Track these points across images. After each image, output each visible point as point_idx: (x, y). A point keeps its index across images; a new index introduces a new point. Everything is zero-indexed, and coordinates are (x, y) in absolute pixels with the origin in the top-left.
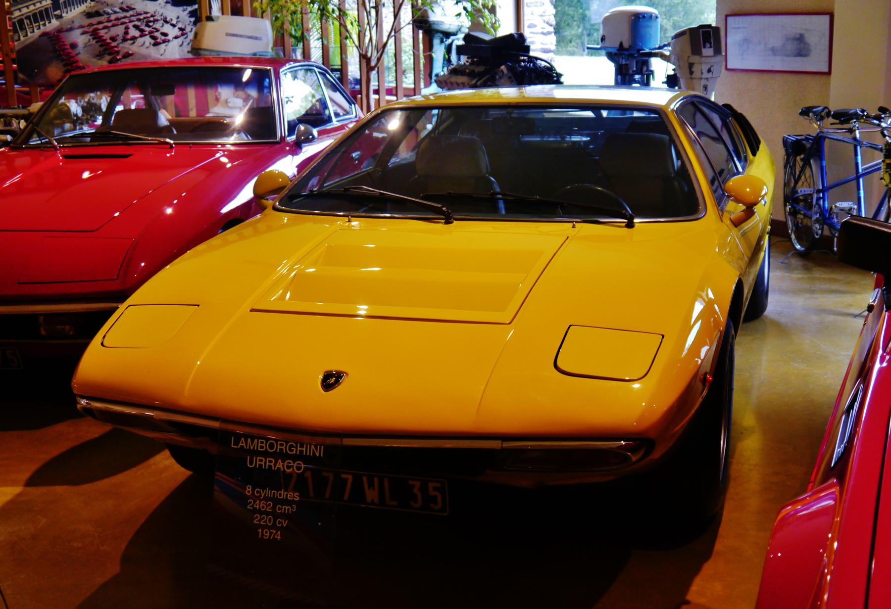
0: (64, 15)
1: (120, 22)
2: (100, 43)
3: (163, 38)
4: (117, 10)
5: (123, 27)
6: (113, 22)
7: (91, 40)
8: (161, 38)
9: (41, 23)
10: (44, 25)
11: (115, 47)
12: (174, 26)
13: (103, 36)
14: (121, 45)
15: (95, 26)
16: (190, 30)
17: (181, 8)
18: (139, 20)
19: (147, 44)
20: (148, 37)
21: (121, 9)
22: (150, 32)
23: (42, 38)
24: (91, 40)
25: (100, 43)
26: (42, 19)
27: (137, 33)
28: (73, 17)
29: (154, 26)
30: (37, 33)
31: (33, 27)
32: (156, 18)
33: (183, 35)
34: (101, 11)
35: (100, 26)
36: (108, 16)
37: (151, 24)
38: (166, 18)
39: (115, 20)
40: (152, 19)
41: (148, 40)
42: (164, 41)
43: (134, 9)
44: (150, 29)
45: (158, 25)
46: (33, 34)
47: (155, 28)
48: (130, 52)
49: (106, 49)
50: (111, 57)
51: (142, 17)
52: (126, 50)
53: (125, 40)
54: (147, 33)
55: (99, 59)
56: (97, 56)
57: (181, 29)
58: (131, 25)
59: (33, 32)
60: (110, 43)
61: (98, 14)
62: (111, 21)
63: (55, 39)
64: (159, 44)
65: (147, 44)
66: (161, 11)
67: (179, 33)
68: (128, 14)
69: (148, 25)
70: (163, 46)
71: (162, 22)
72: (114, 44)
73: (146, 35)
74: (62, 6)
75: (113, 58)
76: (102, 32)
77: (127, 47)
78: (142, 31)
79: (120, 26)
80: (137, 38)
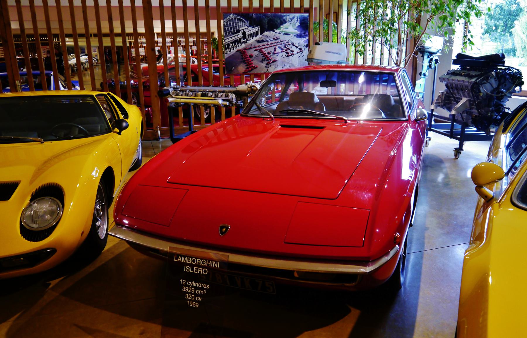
0: (247, 42)
1: (273, 45)
2: (263, 55)
3: (291, 53)
4: (272, 39)
6: (269, 45)
7: (259, 54)
8: (290, 53)
9: (237, 45)
10: (239, 46)
11: (269, 57)
12: (297, 47)
13: (264, 52)
14: (272, 56)
15: (261, 47)
16: (304, 49)
18: (281, 44)
21: (274, 39)
22: (286, 50)
23: (237, 53)
24: (259, 54)
25: (263, 55)
26: (238, 43)
27: (280, 51)
28: (252, 43)
29: (288, 47)
30: (235, 50)
31: (233, 47)
32: (289, 43)
33: (300, 52)
34: (264, 40)
35: (264, 47)
36: (267, 42)
37: (286, 46)
38: (293, 44)
39: (270, 44)
41: (284, 54)
43: (279, 39)
44: (286, 49)
45: (289, 47)
46: (233, 51)
47: (288, 48)
48: (276, 60)
49: (265, 58)
50: (267, 62)
51: (282, 43)
52: (274, 59)
53: (274, 54)
54: (284, 50)
55: (262, 63)
56: (261, 61)
57: (300, 49)
58: (277, 47)
59: (233, 49)
60: (268, 55)
61: (263, 41)
62: (268, 44)
63: (242, 52)
64: (290, 56)
65: (284, 56)
66: (292, 40)
67: (299, 51)
68: (276, 41)
69: (285, 47)
71: (292, 45)
72: (269, 56)
73: (284, 51)
74: (247, 37)
75: (268, 62)
76: (264, 50)
78: (282, 49)
79: (273, 47)
80: (279, 53)
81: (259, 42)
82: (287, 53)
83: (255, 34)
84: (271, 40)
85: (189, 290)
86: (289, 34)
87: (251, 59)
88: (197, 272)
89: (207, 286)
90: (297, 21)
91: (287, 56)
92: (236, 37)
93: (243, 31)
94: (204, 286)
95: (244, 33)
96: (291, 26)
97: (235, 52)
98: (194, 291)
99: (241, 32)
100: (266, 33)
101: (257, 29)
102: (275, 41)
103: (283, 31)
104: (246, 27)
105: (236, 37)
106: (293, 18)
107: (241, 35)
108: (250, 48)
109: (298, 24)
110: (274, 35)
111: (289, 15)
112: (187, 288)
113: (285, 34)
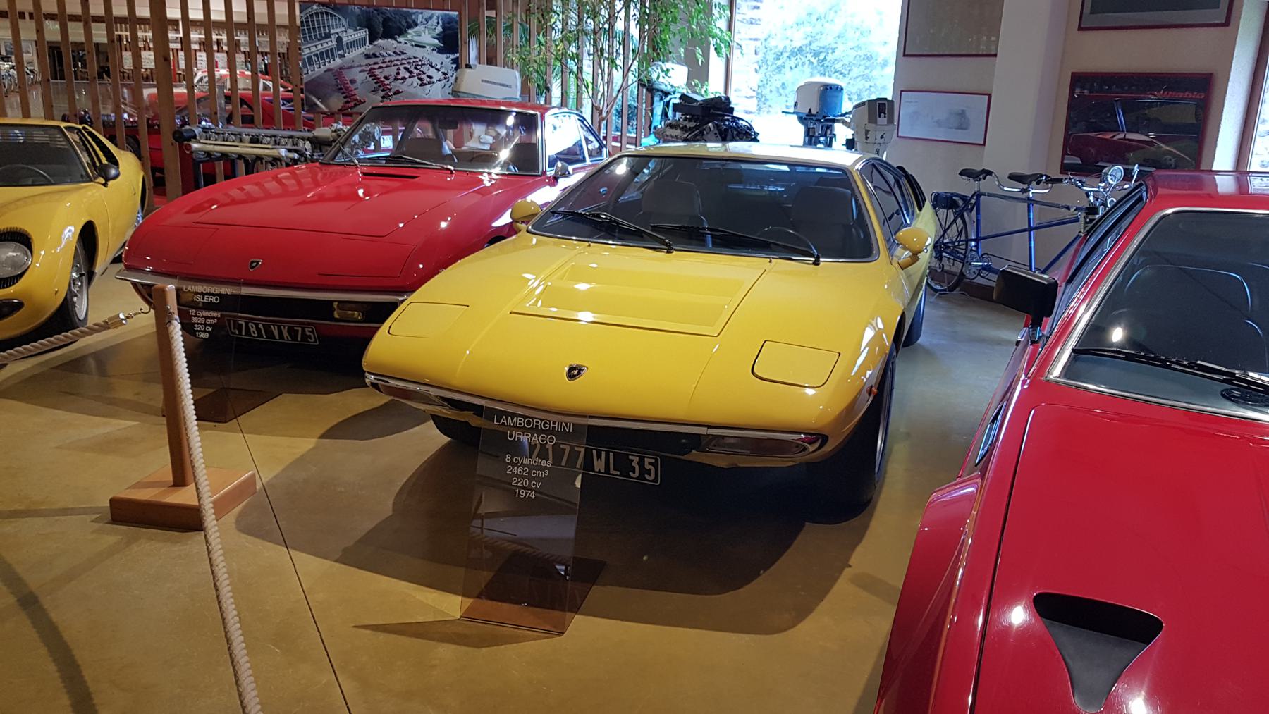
0: (346, 55)
1: (393, 64)
2: (375, 81)
3: (429, 80)
4: (392, 54)
5: (396, 68)
8: (426, 80)
9: (327, 60)
10: (329, 62)
11: (388, 84)
12: (438, 70)
15: (372, 66)
17: (445, 56)
18: (409, 63)
19: (415, 84)
20: (416, 78)
21: (394, 52)
22: (418, 74)
23: (327, 73)
25: (375, 81)
26: (328, 57)
27: (407, 75)
29: (422, 69)
32: (423, 62)
33: (445, 78)
34: (378, 54)
35: (376, 66)
40: (420, 63)
41: (415, 80)
42: (429, 83)
43: (405, 53)
44: (418, 71)
45: (424, 69)
46: (319, 69)
48: (400, 90)
49: (380, 86)
50: (383, 93)
51: (411, 61)
52: (397, 89)
53: (396, 79)
56: (373, 91)
57: (444, 73)
61: (375, 56)
62: (385, 62)
63: (338, 74)
64: (425, 84)
65: (415, 84)
66: (428, 57)
67: (442, 77)
68: (400, 58)
69: (417, 69)
70: (428, 86)
72: (387, 82)
73: (414, 76)
74: (345, 47)
76: (377, 72)
77: (397, 85)
78: (411, 72)
81: (367, 56)
82: (421, 79)
83: (361, 42)
86: (425, 47)
90: (438, 23)
91: (421, 85)
92: (325, 45)
93: (337, 36)
95: (339, 40)
96: (427, 31)
97: (322, 72)
99: (334, 38)
102: (397, 57)
103: (410, 40)
104: (343, 29)
105: (325, 45)
106: (431, 18)
107: (334, 43)
108: (351, 67)
109: (439, 29)
110: (394, 46)
111: (422, 13)
113: (416, 45)
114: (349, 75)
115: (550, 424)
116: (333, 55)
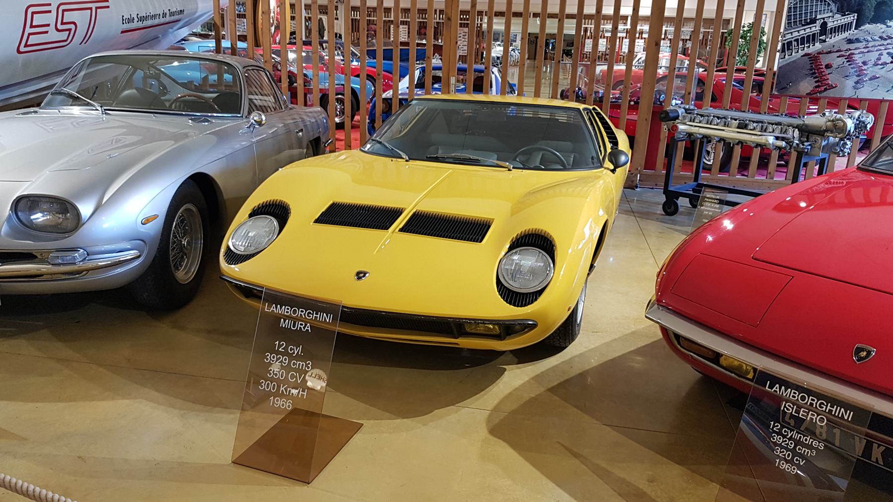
0: (827, 40)
1: (876, 48)
7: (845, 62)
9: (806, 45)
10: (809, 47)
11: (865, 70)
15: (852, 51)
21: (881, 37)
23: (802, 57)
24: (845, 62)
26: (808, 42)
30: (801, 53)
31: (798, 48)
36: (867, 43)
39: (872, 47)
48: (877, 76)
52: (874, 74)
53: (876, 65)
59: (798, 52)
60: (862, 66)
63: (814, 59)
68: (885, 43)
72: (865, 67)
74: (828, 32)
79: (876, 52)
81: (850, 41)
83: (846, 27)
84: (874, 40)
85: (783, 442)
87: (828, 71)
88: (797, 415)
89: (819, 445)
92: (808, 30)
93: (822, 21)
94: (814, 443)
95: (824, 25)
97: (800, 56)
98: (793, 445)
99: (819, 23)
100: (867, 27)
101: (852, 18)
102: (883, 42)
104: (831, 14)
105: (808, 30)
107: (818, 28)
108: (830, 52)
110: (883, 30)
112: (780, 439)
114: (825, 60)
115: (827, 406)
116: (814, 40)
